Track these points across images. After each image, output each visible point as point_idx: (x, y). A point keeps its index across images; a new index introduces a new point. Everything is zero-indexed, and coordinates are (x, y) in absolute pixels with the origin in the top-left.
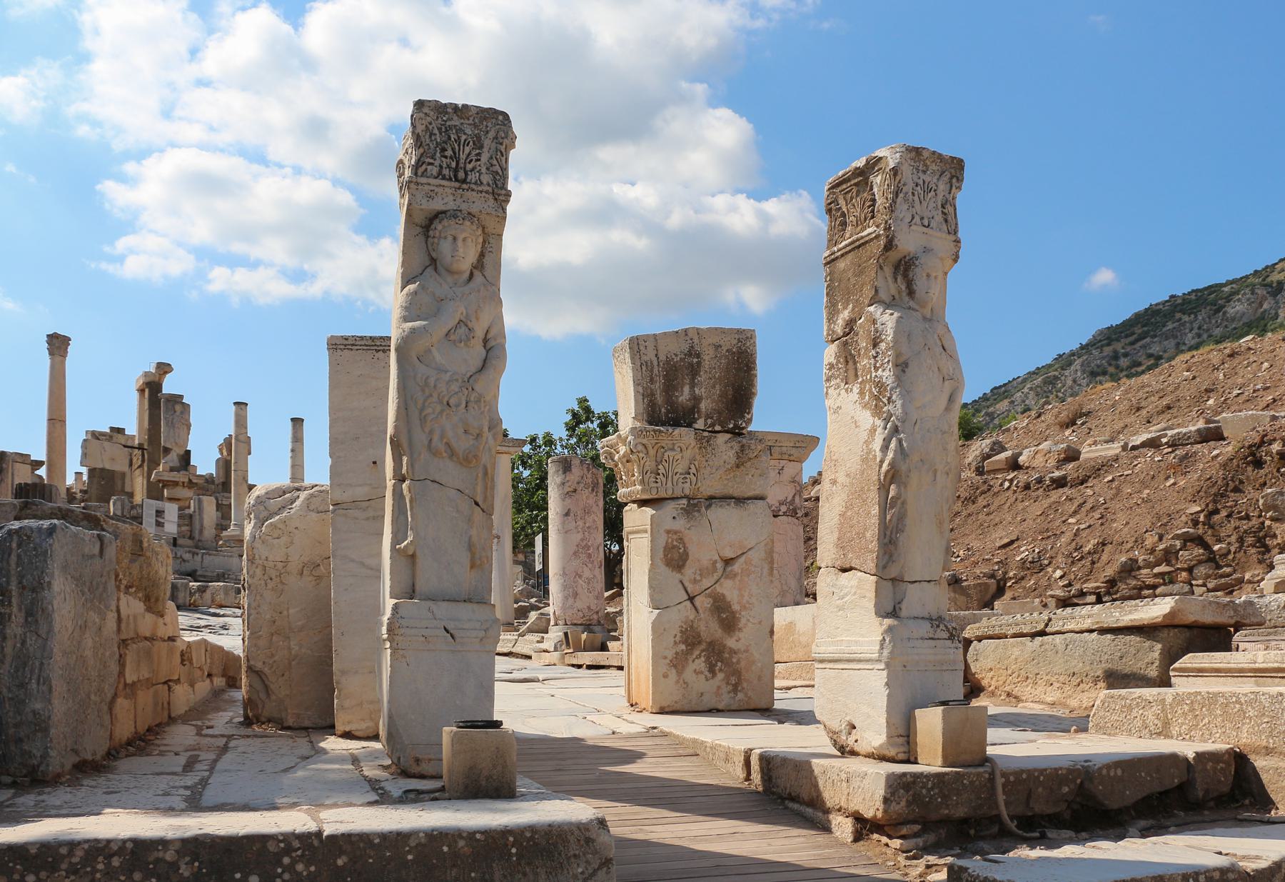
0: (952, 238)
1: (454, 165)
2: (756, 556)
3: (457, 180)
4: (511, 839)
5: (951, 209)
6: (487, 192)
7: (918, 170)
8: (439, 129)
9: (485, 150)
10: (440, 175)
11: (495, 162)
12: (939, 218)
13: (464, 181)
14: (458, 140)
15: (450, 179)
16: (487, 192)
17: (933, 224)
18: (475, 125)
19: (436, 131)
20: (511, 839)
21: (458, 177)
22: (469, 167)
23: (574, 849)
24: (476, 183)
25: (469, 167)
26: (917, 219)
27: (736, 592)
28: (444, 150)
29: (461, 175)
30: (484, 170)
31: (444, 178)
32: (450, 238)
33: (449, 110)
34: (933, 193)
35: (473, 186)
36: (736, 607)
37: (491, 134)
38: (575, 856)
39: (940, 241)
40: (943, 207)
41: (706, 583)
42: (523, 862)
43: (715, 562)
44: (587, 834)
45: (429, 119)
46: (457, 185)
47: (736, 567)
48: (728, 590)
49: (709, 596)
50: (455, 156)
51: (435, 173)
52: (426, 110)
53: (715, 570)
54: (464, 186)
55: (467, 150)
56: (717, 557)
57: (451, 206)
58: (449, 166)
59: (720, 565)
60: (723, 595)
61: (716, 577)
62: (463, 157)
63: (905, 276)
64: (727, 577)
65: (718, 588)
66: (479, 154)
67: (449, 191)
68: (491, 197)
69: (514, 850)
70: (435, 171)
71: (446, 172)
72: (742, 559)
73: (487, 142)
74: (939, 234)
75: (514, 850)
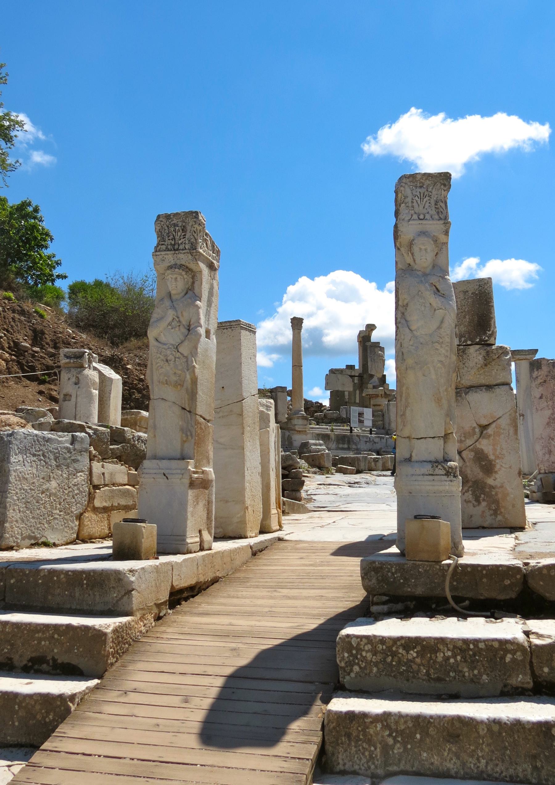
0: (442, 222)
1: (173, 243)
2: (504, 422)
3: (174, 250)
4: (84, 576)
5: (443, 205)
6: (187, 253)
7: (416, 187)
8: (168, 227)
9: (188, 232)
10: (167, 249)
11: (192, 237)
12: (433, 212)
13: (178, 250)
14: (175, 231)
15: (171, 250)
16: (187, 253)
17: (428, 216)
18: (183, 221)
19: (166, 228)
20: (84, 576)
21: (175, 248)
22: (180, 242)
23: (113, 583)
24: (183, 250)
25: (180, 242)
26: (415, 217)
27: (491, 447)
28: (169, 237)
29: (176, 247)
30: (187, 242)
31: (169, 250)
32: (170, 279)
33: (172, 217)
34: (427, 198)
35: (181, 251)
36: (492, 457)
37: (190, 224)
38: (113, 587)
39: (433, 226)
40: (436, 205)
41: (469, 442)
42: (89, 588)
43: (475, 428)
44: (119, 576)
45: (162, 223)
46: (173, 252)
47: (490, 431)
48: (485, 445)
49: (472, 450)
50: (174, 239)
51: (164, 249)
52: (161, 219)
53: (474, 433)
54: (177, 252)
55: (179, 234)
56: (475, 425)
57: (173, 262)
58: (171, 244)
59: (477, 430)
60: (482, 450)
61: (476, 437)
62: (177, 238)
63: (410, 251)
64: (484, 438)
65: (478, 445)
66: (185, 235)
67: (170, 255)
68: (189, 255)
69: (85, 582)
70: (164, 247)
71: (169, 247)
72: (493, 426)
73: (189, 228)
74: (431, 222)
75: (85, 582)
